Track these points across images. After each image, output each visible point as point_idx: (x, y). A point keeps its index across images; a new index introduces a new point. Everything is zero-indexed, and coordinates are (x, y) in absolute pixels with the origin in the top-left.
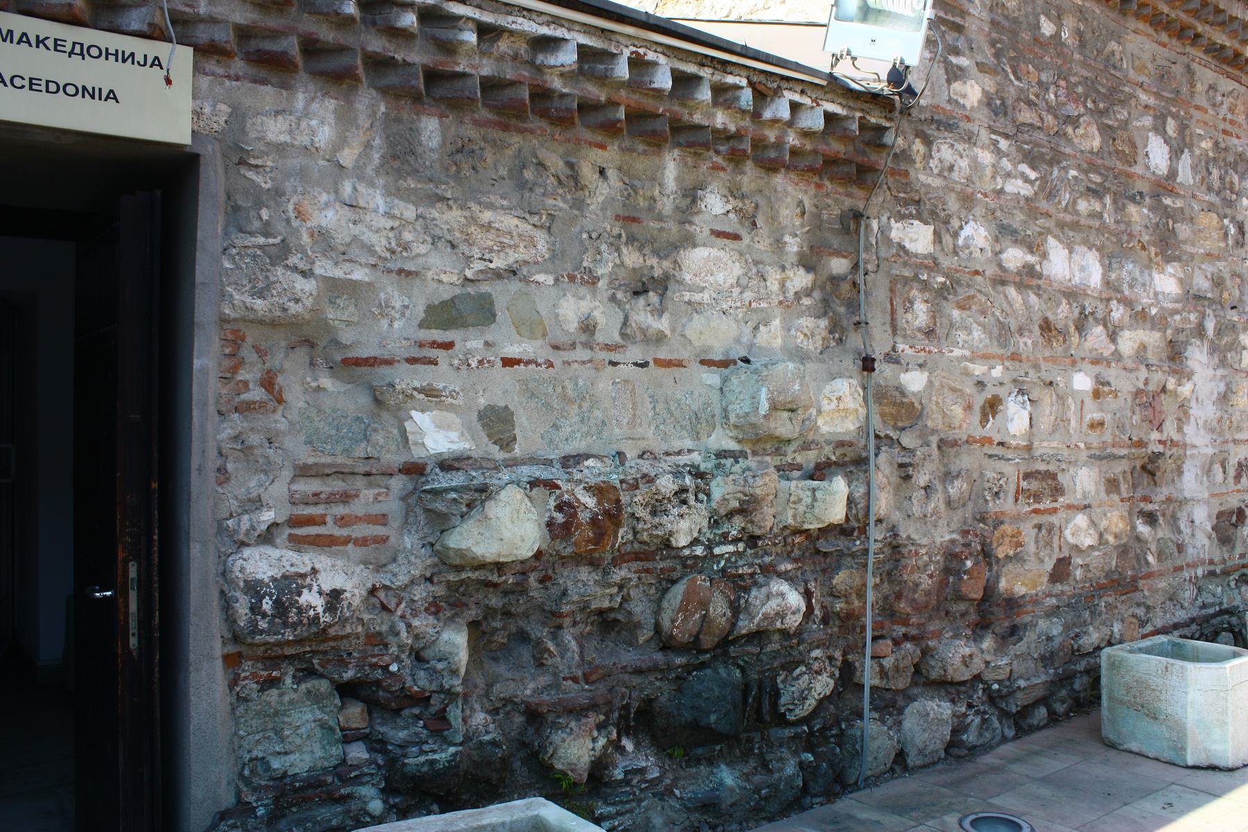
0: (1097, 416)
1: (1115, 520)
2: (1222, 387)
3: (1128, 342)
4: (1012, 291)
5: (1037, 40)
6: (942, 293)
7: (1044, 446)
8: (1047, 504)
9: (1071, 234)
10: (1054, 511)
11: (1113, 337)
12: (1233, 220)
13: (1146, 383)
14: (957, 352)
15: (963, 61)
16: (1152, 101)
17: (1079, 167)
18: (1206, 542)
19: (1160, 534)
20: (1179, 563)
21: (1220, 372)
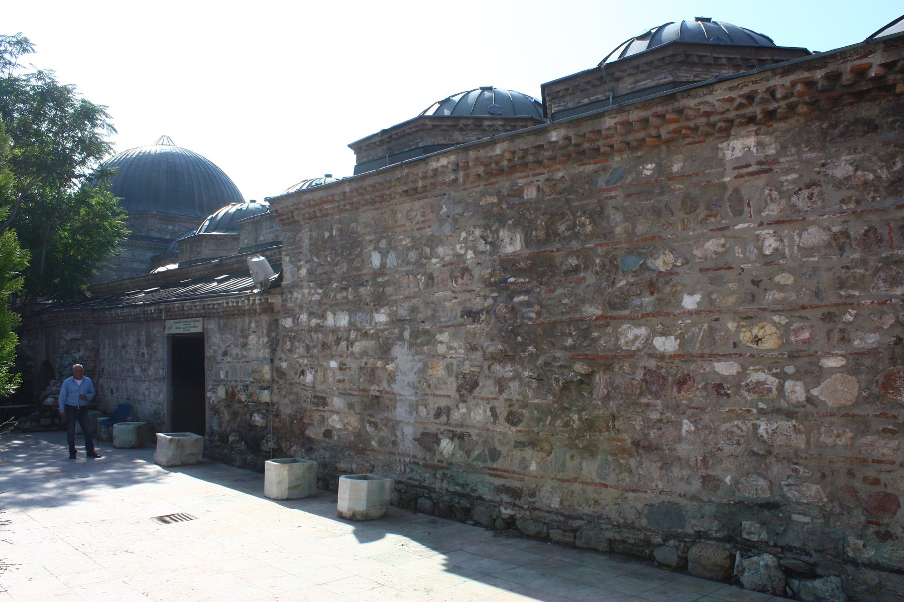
0: (341, 377)
1: (354, 421)
2: (420, 365)
3: (357, 347)
4: (313, 334)
5: (324, 242)
6: (295, 337)
7: (320, 387)
8: (321, 408)
9: (335, 308)
10: (324, 411)
11: (352, 344)
12: (424, 274)
13: (366, 363)
14: (295, 356)
15: (302, 263)
16: (372, 237)
17: (338, 282)
18: (410, 445)
19: (382, 434)
20: (392, 451)
21: (416, 357)
